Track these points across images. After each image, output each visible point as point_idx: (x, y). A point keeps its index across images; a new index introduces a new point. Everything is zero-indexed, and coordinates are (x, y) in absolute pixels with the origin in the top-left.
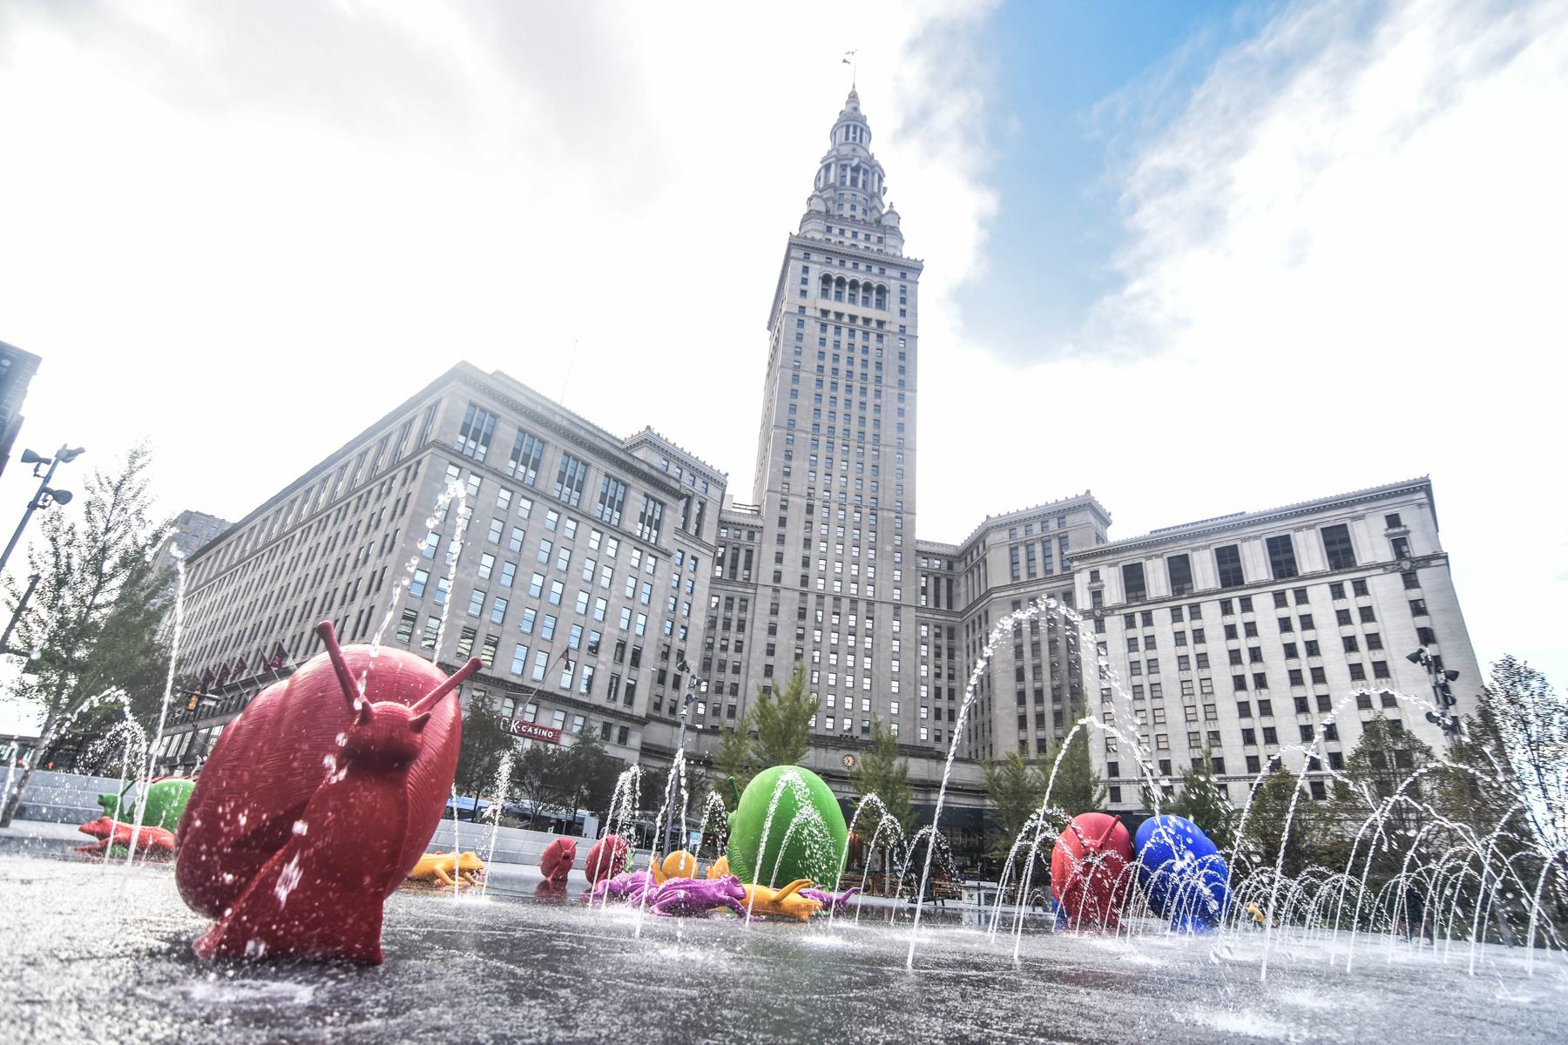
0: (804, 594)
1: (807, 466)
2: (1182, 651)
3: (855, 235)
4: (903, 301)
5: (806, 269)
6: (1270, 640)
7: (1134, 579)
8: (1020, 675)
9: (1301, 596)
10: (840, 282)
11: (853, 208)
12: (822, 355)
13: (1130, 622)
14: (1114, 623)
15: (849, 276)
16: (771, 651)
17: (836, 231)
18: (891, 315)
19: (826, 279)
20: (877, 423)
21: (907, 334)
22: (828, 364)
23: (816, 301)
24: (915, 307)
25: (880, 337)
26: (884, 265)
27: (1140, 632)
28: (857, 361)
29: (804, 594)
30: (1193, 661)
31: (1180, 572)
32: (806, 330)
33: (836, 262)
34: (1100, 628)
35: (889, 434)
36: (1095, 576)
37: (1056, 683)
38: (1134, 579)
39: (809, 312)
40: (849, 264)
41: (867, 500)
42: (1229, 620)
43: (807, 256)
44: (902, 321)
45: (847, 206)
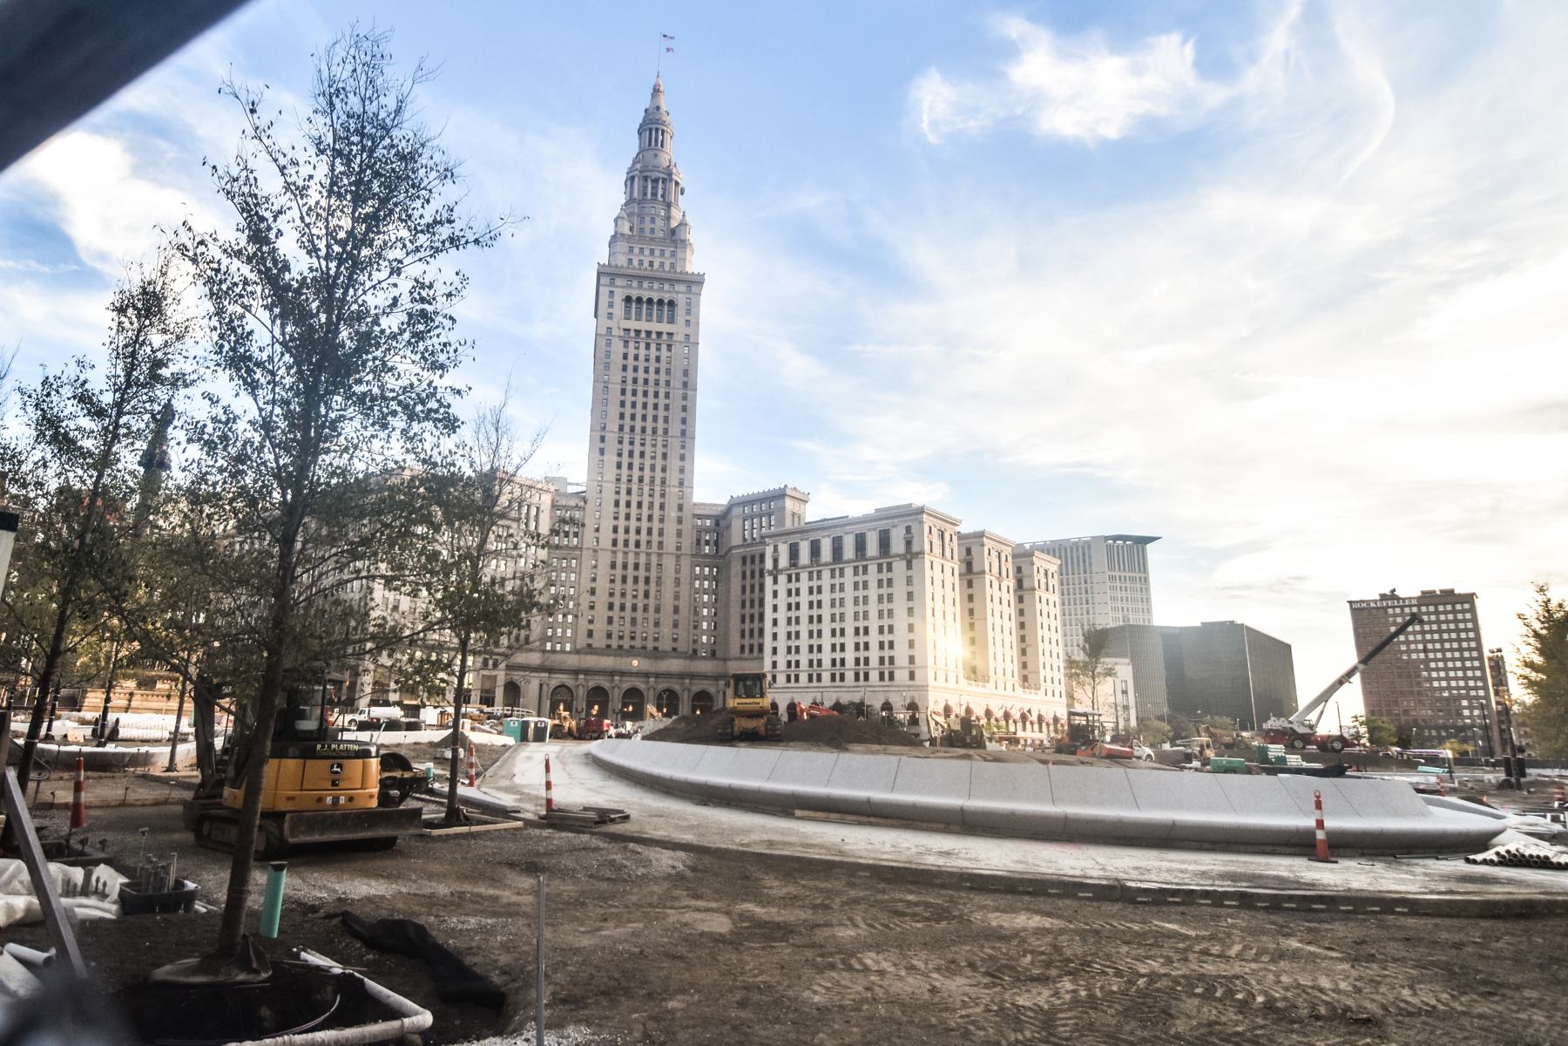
0: (614, 552)
1: (615, 459)
3: (652, 251)
4: (688, 312)
5: (612, 292)
6: (849, 594)
7: (794, 553)
8: (743, 606)
9: (865, 568)
10: (639, 300)
11: (653, 220)
12: (625, 368)
14: (782, 578)
15: (646, 295)
16: (593, 592)
18: (678, 329)
19: (628, 299)
20: (666, 420)
21: (691, 342)
22: (630, 374)
23: (620, 322)
24: (697, 317)
25: (669, 347)
26: (672, 281)
27: (793, 586)
28: (652, 370)
29: (614, 552)
31: (815, 550)
32: (613, 348)
33: (635, 284)
35: (675, 428)
36: (776, 549)
39: (615, 332)
40: (645, 284)
41: (658, 481)
43: (612, 283)
44: (687, 331)
45: (648, 219)
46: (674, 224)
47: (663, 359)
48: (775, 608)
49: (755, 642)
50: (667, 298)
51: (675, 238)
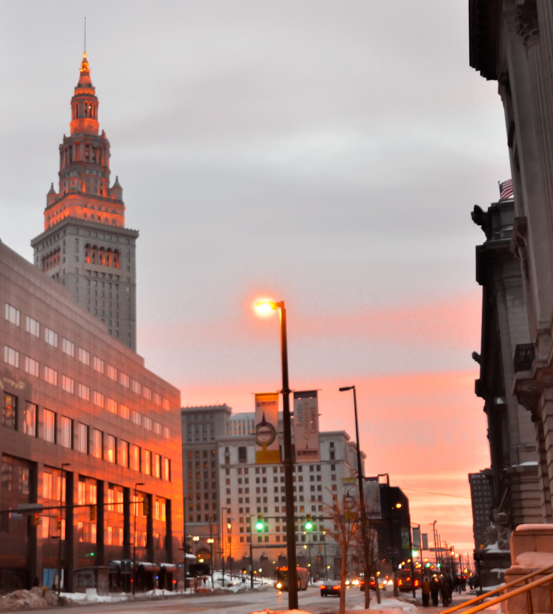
2: (258, 485)
7: (242, 453)
10: (95, 247)
13: (239, 472)
14: (233, 472)
15: (100, 244)
17: (89, 206)
18: (122, 271)
19: (87, 246)
25: (117, 285)
27: (243, 477)
30: (262, 490)
34: (228, 472)
36: (227, 450)
37: (206, 491)
38: (242, 453)
39: (81, 272)
42: (276, 475)
46: (111, 186)
47: (114, 295)
48: (228, 491)
49: (203, 512)
50: (114, 247)
51: (114, 199)
